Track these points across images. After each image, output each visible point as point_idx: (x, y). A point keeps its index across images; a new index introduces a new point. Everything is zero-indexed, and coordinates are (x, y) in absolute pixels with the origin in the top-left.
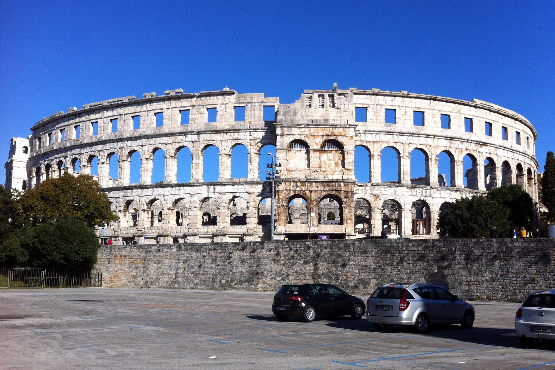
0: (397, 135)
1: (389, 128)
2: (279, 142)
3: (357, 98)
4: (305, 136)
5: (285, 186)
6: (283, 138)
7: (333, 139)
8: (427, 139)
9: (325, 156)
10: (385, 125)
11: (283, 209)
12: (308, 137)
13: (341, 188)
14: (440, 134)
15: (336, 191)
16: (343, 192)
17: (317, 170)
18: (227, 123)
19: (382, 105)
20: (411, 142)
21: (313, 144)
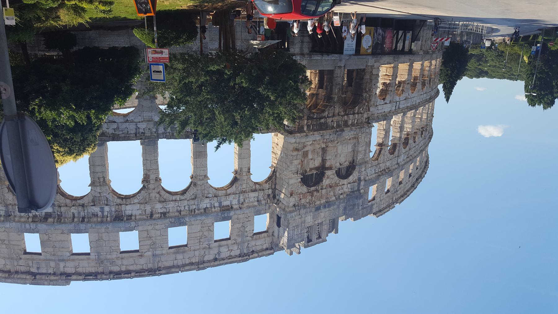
0: (214, 207)
1: (226, 215)
2: (362, 172)
3: (266, 243)
4: (339, 185)
5: (362, 119)
6: (358, 177)
7: (312, 188)
8: (164, 210)
9: (317, 162)
11: (367, 88)
13: (307, 123)
14: (140, 223)
15: (312, 118)
16: (306, 117)
17: (330, 145)
18: (381, 180)
19: (234, 243)
20: (192, 202)
21: (331, 177)
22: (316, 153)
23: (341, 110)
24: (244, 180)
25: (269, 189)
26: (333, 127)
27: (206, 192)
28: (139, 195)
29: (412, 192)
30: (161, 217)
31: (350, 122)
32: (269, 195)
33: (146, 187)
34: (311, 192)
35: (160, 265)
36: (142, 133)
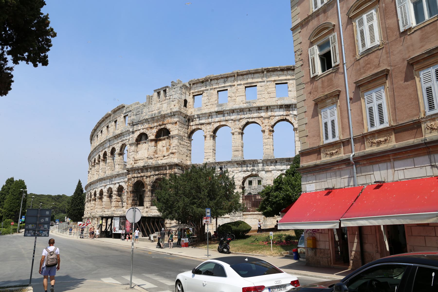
0: (228, 114)
1: (220, 108)
3: (195, 88)
4: (146, 129)
8: (259, 111)
9: (160, 144)
10: (217, 106)
12: (148, 130)
15: (164, 174)
16: (168, 175)
17: (152, 157)
18: (120, 129)
22: (161, 151)
23: (145, 180)
24: (209, 132)
25: (193, 125)
26: (150, 168)
27: (233, 124)
28: (275, 122)
29: (100, 120)
30: (261, 107)
31: (140, 171)
32: (193, 121)
33: (270, 127)
34: (164, 124)
35: (262, 75)
36: (272, 163)
